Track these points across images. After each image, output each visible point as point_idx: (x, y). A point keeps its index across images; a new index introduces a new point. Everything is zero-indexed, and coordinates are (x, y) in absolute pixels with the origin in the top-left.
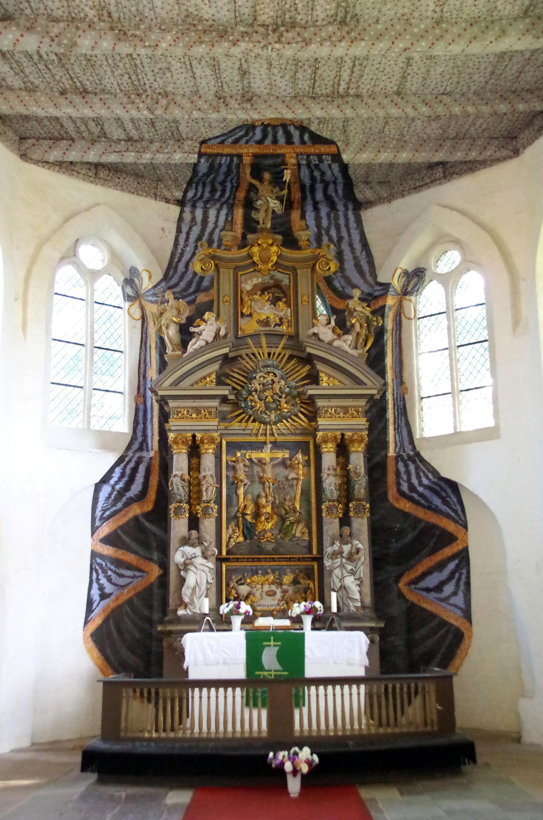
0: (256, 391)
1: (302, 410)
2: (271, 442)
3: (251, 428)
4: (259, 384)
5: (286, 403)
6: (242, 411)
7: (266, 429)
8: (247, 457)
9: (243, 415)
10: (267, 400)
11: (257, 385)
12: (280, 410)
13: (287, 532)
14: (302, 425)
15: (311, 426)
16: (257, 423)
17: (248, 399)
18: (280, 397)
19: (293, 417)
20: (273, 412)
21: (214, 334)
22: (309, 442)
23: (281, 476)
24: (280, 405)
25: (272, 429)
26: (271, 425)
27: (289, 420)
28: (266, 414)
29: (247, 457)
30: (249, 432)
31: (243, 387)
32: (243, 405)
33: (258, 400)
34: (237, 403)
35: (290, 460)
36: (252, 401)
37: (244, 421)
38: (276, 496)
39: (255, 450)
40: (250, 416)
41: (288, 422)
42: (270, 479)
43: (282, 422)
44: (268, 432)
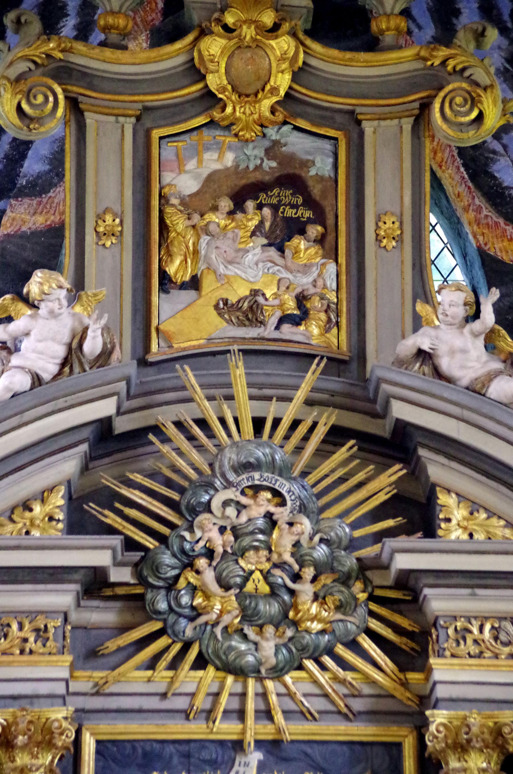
0: (210, 553)
1: (374, 625)
2: (259, 744)
3: (191, 688)
4: (222, 530)
5: (316, 597)
6: (157, 626)
7: (243, 695)
9: (162, 642)
10: (250, 587)
11: (214, 534)
12: (295, 624)
14: (374, 683)
15: (405, 684)
16: (211, 670)
17: (182, 583)
18: (296, 577)
19: (340, 649)
20: (270, 630)
21: (61, 351)
22: (398, 746)
24: (294, 606)
25: (264, 695)
26: (260, 679)
27: (327, 660)
28: (245, 637)
30: (181, 703)
31: (162, 539)
32: (163, 606)
33: (214, 587)
34: (141, 597)
36: (193, 589)
37: (163, 663)
40: (187, 646)
41: (323, 667)
43: (301, 667)
44: (251, 706)
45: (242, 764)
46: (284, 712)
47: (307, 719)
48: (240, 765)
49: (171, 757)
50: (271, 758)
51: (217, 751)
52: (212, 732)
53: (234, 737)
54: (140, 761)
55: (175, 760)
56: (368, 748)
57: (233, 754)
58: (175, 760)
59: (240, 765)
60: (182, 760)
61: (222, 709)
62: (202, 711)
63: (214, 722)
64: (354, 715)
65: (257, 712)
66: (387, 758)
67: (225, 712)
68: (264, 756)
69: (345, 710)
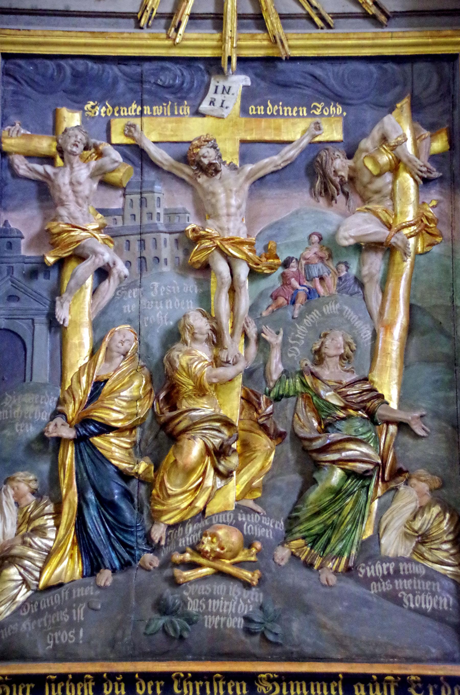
8: (118, 138)
13: (334, 527)
23: (302, 236)
29: (118, 138)
35: (350, 156)
38: (269, 336)
39: (162, 100)
42: (238, 244)
45: (220, 90)
46: (282, 17)
47: (316, 26)
48: (216, 92)
49: (115, 82)
50: (263, 84)
51: (182, 74)
52: (175, 45)
53: (208, 53)
54: (68, 84)
55: (121, 86)
56: (407, 67)
57: (206, 78)
58: (121, 86)
59: (216, 92)
60: (132, 85)
61: (188, 11)
62: (160, 16)
63: (177, 30)
64: (388, 17)
65: (240, 17)
66: (435, 78)
67: (192, 17)
68: (252, 81)
69: (373, 10)
